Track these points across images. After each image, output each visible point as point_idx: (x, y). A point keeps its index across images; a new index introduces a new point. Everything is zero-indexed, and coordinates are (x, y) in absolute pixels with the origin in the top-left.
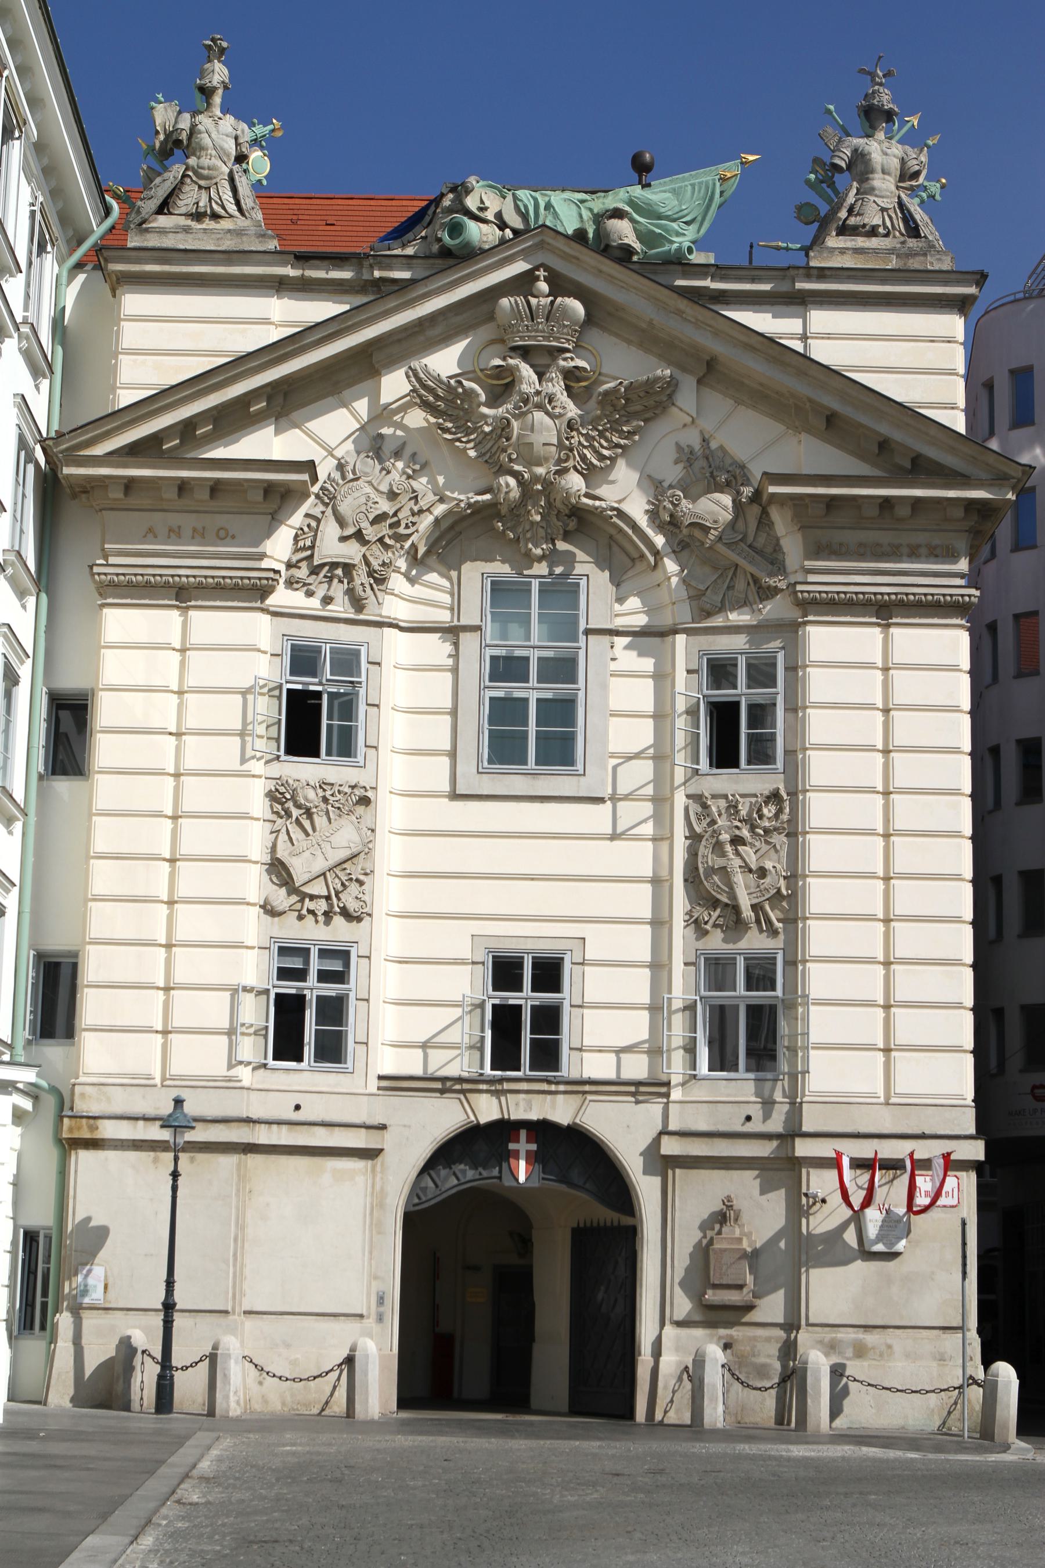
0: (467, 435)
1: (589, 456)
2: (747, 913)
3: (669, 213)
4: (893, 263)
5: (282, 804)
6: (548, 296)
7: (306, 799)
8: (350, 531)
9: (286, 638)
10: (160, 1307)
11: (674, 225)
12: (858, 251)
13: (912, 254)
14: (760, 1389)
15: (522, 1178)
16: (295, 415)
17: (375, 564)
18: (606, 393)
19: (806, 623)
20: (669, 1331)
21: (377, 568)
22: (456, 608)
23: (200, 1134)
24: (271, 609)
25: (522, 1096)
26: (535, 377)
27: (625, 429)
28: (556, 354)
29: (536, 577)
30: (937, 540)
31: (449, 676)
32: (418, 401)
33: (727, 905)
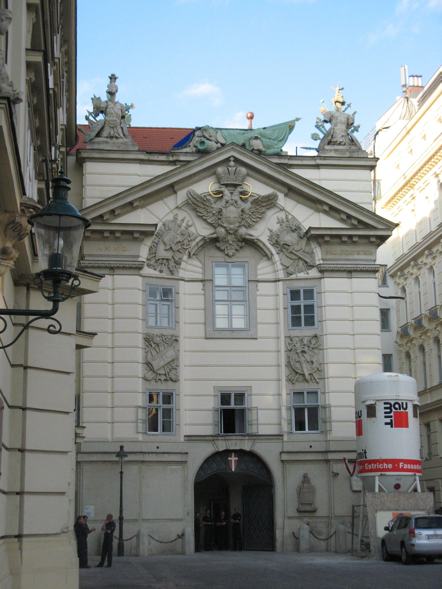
0: (207, 214)
1: (248, 221)
2: (307, 377)
3: (274, 137)
4: (348, 155)
5: (148, 342)
6: (235, 166)
7: (157, 341)
8: (168, 247)
9: (147, 285)
10: (118, 519)
11: (275, 142)
12: (336, 150)
13: (354, 152)
14: (318, 539)
15: (233, 470)
17: (176, 259)
18: (255, 200)
19: (323, 278)
20: (287, 521)
21: (177, 260)
22: (204, 273)
23: (130, 458)
24: (142, 275)
25: (234, 441)
26: (229, 195)
27: (261, 212)
28: (237, 186)
29: (230, 262)
31: (203, 297)
32: (190, 202)
33: (300, 374)
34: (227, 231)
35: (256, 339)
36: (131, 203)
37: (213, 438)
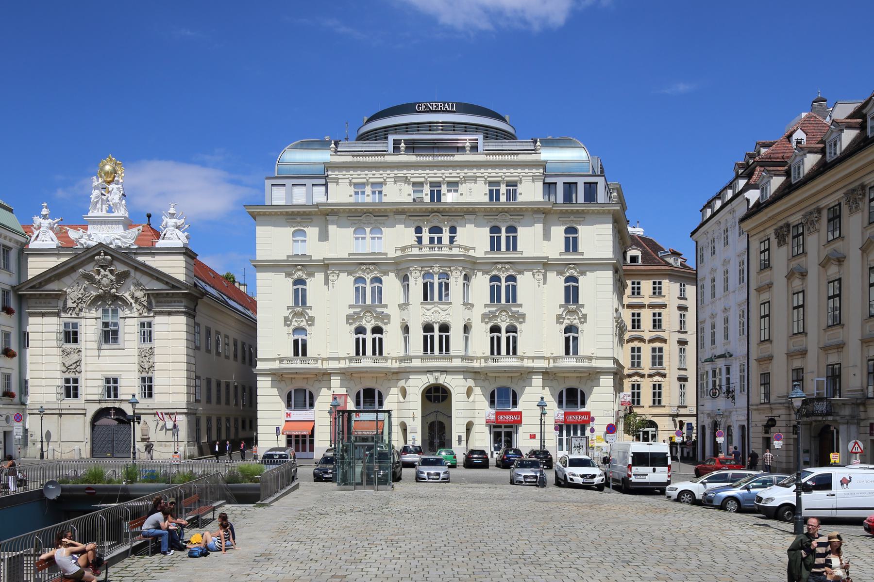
16: (63, 279)
30: (179, 299)
34: (104, 291)
35: (123, 349)
36: (50, 278)
37: (100, 401)
